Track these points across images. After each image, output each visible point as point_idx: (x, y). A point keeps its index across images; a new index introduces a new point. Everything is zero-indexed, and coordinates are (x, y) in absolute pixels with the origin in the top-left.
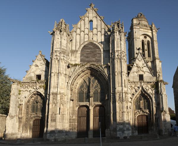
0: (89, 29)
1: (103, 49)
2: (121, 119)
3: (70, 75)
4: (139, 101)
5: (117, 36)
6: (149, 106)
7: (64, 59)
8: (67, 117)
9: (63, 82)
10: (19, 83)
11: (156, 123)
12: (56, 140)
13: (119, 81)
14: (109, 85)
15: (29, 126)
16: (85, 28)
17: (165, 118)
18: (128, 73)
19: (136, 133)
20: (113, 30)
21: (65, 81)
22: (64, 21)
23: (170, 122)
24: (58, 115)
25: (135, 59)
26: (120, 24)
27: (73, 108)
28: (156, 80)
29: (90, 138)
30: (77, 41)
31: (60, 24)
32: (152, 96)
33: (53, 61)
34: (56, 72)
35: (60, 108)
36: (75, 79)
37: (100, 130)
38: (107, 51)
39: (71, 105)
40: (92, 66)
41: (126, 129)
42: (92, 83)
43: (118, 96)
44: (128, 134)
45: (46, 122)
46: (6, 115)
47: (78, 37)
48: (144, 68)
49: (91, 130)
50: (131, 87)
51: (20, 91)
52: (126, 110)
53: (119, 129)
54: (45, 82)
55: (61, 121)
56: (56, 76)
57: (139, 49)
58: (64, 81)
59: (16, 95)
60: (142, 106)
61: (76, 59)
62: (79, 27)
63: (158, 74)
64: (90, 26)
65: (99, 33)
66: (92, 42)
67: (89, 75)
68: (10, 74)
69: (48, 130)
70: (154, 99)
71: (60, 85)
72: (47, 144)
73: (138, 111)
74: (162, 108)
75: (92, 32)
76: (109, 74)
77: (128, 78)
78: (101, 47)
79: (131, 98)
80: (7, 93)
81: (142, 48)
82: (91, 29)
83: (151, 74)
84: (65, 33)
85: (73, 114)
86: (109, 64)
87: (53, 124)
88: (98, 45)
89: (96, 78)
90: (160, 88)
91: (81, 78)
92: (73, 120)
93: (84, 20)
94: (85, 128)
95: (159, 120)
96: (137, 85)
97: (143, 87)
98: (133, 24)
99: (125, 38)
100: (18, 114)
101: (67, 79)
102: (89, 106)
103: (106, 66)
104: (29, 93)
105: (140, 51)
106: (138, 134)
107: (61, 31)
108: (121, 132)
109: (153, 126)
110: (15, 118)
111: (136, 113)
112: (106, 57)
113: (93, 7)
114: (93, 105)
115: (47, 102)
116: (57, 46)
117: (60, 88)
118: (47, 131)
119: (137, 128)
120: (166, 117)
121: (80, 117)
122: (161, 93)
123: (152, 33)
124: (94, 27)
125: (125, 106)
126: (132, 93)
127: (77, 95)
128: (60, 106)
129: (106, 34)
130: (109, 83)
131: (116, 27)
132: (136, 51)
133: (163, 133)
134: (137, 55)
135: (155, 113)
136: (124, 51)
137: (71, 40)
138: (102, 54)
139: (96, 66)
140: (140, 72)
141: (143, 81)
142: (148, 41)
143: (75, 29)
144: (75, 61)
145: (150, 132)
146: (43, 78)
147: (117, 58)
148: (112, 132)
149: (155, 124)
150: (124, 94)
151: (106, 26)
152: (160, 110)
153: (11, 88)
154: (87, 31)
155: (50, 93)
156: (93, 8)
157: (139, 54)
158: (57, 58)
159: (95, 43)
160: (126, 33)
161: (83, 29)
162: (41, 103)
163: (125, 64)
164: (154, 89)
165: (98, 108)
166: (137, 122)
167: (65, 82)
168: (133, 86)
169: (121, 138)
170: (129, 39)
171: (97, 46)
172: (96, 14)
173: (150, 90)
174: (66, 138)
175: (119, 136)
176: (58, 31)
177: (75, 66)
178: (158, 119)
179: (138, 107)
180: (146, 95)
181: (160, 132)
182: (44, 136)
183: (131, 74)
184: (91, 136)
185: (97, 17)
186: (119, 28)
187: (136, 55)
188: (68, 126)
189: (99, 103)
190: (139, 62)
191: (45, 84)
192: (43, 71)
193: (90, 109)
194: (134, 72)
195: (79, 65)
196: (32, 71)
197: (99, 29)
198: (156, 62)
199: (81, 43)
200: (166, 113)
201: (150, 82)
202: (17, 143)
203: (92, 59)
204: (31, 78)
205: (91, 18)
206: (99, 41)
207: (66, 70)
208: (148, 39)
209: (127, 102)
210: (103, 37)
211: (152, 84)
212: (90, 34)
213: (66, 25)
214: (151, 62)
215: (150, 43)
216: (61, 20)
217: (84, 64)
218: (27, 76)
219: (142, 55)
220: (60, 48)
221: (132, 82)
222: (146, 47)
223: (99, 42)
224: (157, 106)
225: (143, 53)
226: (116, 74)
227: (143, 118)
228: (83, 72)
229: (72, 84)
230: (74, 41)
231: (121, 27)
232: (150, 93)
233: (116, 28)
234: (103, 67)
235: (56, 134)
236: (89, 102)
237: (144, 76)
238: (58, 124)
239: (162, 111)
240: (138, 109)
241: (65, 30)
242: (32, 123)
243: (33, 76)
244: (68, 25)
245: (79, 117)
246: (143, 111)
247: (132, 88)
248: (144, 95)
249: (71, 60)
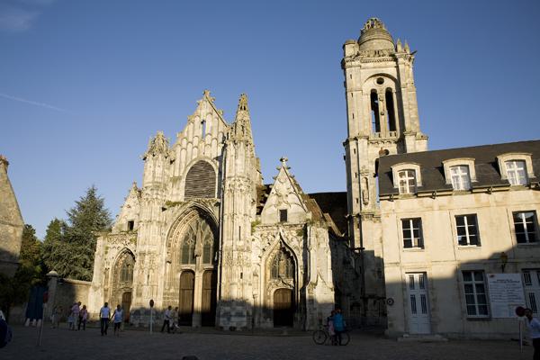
27: (171, 273)
36: (174, 227)
49: (197, 312)
51: (107, 248)
60: (282, 271)
61: (178, 193)
82: (204, 136)
83: (303, 207)
85: (170, 285)
88: (212, 163)
92: (173, 294)
110: (99, 290)
114: (200, 268)
119: (272, 313)
124: (206, 132)
144: (178, 195)
145: (295, 324)
154: (196, 143)
159: (206, 160)
161: (190, 139)
171: (210, 165)
173: (295, 240)
179: (275, 274)
184: (196, 322)
195: (180, 203)
204: (122, 225)
230: (177, 162)
242: (120, 297)
248: (285, 250)
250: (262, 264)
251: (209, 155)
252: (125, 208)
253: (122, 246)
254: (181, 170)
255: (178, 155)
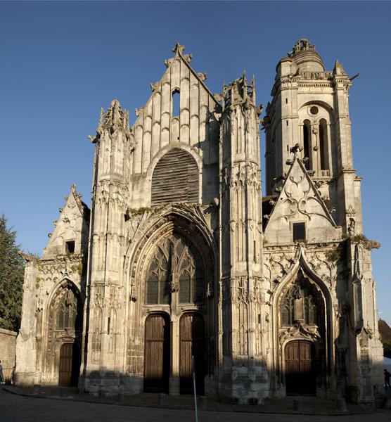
0: (171, 115)
1: (203, 161)
2: (242, 349)
3: (130, 238)
4: (293, 301)
5: (237, 120)
6: (319, 315)
7: (118, 199)
8: (123, 340)
9: (116, 255)
10: (38, 261)
11: (338, 367)
12: (103, 393)
13: (240, 247)
14: (216, 257)
15: (53, 358)
16: (163, 112)
17: (366, 351)
18: (265, 223)
19: (282, 392)
20: (228, 104)
21: (121, 251)
22: (118, 105)
23: (384, 366)
24: (106, 335)
25: (283, 178)
26: (245, 84)
27: (136, 318)
28: (343, 237)
29: (173, 394)
30: (145, 149)
31: (111, 114)
32: (328, 285)
33: (97, 207)
34: (103, 233)
35: (109, 319)
37: (194, 377)
38: (211, 167)
39: (131, 312)
40: (178, 210)
41: (254, 378)
42: (176, 254)
43: (238, 286)
44: (261, 392)
45: (83, 349)
46: (16, 333)
47: (147, 136)
48: (308, 202)
49: (176, 377)
50: (271, 260)
52: (257, 326)
53: (238, 377)
54: (83, 258)
55: (110, 351)
56: (102, 242)
57: (294, 150)
58: (118, 254)
59: (31, 289)
60: (299, 315)
61: (142, 197)
62: (149, 112)
63: (348, 218)
64: (173, 106)
65: (194, 120)
66: (178, 147)
67: (169, 235)
68: (24, 243)
69: (87, 369)
70: (333, 294)
71: (111, 264)
72: (86, 402)
73: (289, 330)
74: (358, 322)
75: (178, 120)
76: (217, 229)
77: (263, 237)
78: (198, 156)
79: (269, 292)
80: (17, 285)
81: (303, 146)
82: (177, 111)
83: (329, 219)
84: (120, 135)
86: (217, 201)
87: (97, 354)
88: (192, 152)
89: (186, 241)
90: (355, 259)
91: (153, 242)
92: (136, 347)
93: (160, 93)
94: (160, 369)
95: (347, 356)
96: (287, 254)
97: (305, 259)
98: (279, 79)
99: (259, 121)
100: (35, 330)
101: (125, 248)
102: (169, 313)
103: (210, 207)
104: (53, 283)
105: (298, 153)
106: (287, 395)
107: (112, 132)
108: (242, 387)
109: (330, 375)
110: (30, 340)
111: (284, 333)
112: (209, 183)
113: (181, 54)
114: (179, 309)
115: (86, 303)
116: (104, 168)
117: (110, 271)
118: (85, 370)
120: (369, 348)
121: (150, 341)
122: (355, 274)
123: (335, 94)
125: (255, 315)
126: (274, 277)
127: (143, 287)
128: (110, 313)
129: (211, 120)
130: (215, 253)
131: (235, 95)
132: (287, 156)
133: (360, 399)
134: (290, 166)
135: (337, 335)
136: (255, 160)
137: (133, 150)
138: (201, 176)
139: (186, 210)
140: (296, 216)
141: (305, 242)
142: (323, 121)
143: (140, 121)
144: (141, 200)
146: (78, 248)
147: (236, 183)
148: (220, 384)
149: (336, 368)
150: (252, 282)
151: (210, 97)
152: (352, 328)
153: (24, 274)
154: (165, 122)
155: (92, 284)
156: (180, 56)
157: (296, 164)
158: (105, 199)
159: (183, 148)
160: (261, 108)
161: (157, 118)
162: (74, 308)
163: (257, 197)
164: (335, 263)
165: (189, 319)
166: (284, 359)
167: (120, 256)
168: (277, 257)
169: (241, 402)
170: (267, 125)
171: (189, 156)
172: (188, 71)
173: (324, 267)
174: (121, 390)
175: (238, 397)
176: (107, 131)
177: (140, 214)
178: (345, 352)
179: (289, 319)
180: (312, 282)
181: (349, 393)
182: (80, 382)
183: (272, 225)
184: (174, 390)
185: (188, 79)
186: (242, 97)
187: (286, 168)
188: (125, 363)
189: (192, 307)
190: (296, 187)
191: (82, 261)
192: (77, 233)
193: (172, 322)
194: (279, 219)
196: (59, 234)
197: (194, 111)
198: (345, 183)
199: (154, 154)
200: (371, 338)
201: (325, 245)
202: (35, 394)
203: (176, 193)
204: (57, 249)
205: (176, 84)
206: (195, 141)
207: (122, 225)
208: (323, 114)
209: (259, 305)
210: (203, 129)
211: (331, 248)
212: (173, 126)
213: (121, 113)
214: (328, 183)
215: (329, 127)
216: (113, 103)
217: (159, 207)
218: (49, 245)
219: (304, 165)
220: (111, 173)
221: (273, 247)
222: (315, 140)
223: (194, 146)
224: (342, 314)
225: (307, 158)
226: (233, 225)
227: (302, 348)
228: (158, 227)
229: (134, 259)
230: (138, 151)
231: (248, 94)
232: (324, 278)
233: (235, 99)
234: (202, 210)
235: (102, 380)
236: (170, 303)
237: (309, 226)
238: (106, 355)
239: (358, 331)
240: (289, 323)
241: (121, 125)
242: (58, 351)
243: (60, 243)
244: (127, 113)
245: (148, 341)
246: (302, 331)
247: (273, 263)
248: (307, 283)
249: (132, 200)
250: (274, 303)
251: (187, 141)
252: (61, 223)
253: (61, 277)
254: (144, 163)
255: (140, 141)
